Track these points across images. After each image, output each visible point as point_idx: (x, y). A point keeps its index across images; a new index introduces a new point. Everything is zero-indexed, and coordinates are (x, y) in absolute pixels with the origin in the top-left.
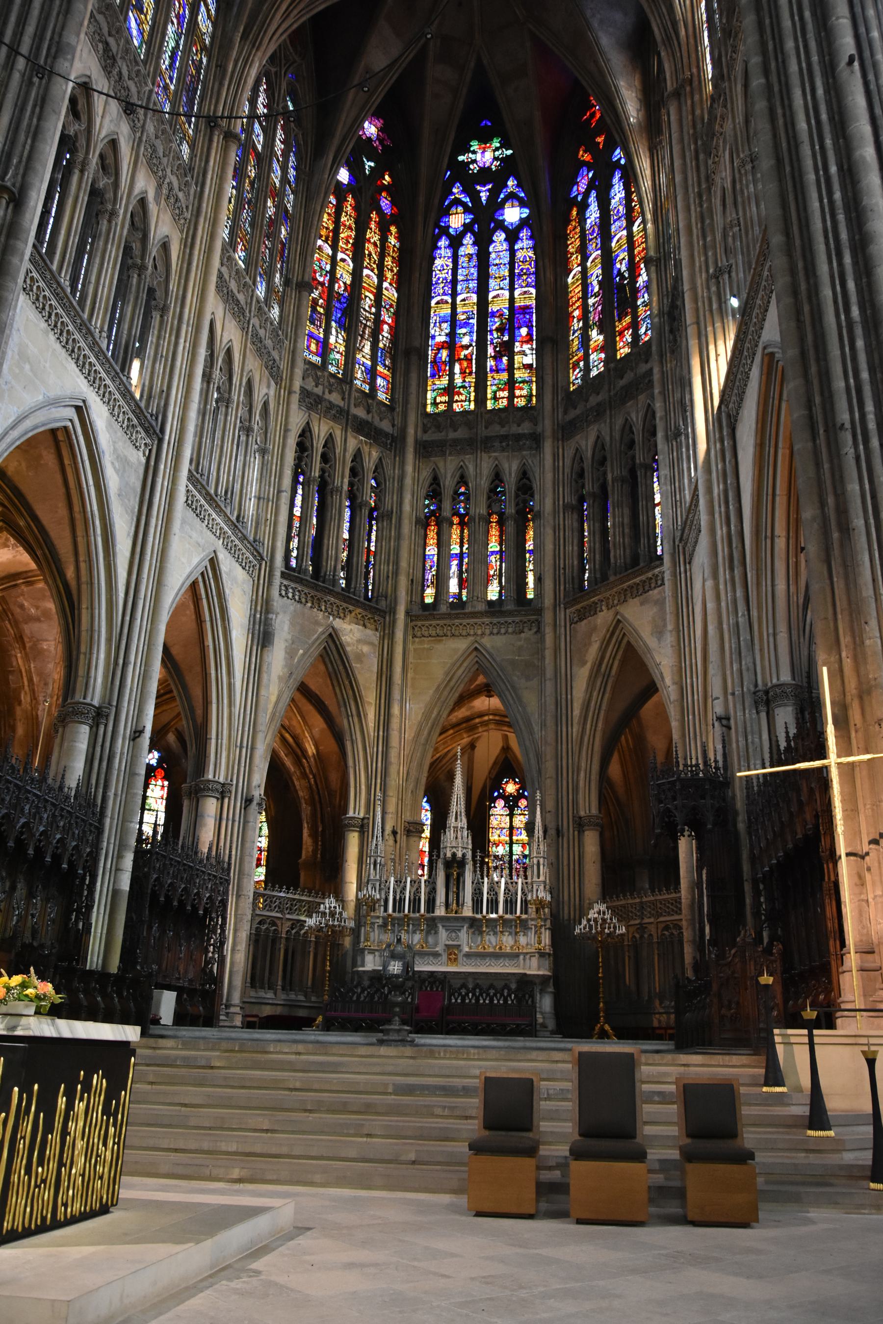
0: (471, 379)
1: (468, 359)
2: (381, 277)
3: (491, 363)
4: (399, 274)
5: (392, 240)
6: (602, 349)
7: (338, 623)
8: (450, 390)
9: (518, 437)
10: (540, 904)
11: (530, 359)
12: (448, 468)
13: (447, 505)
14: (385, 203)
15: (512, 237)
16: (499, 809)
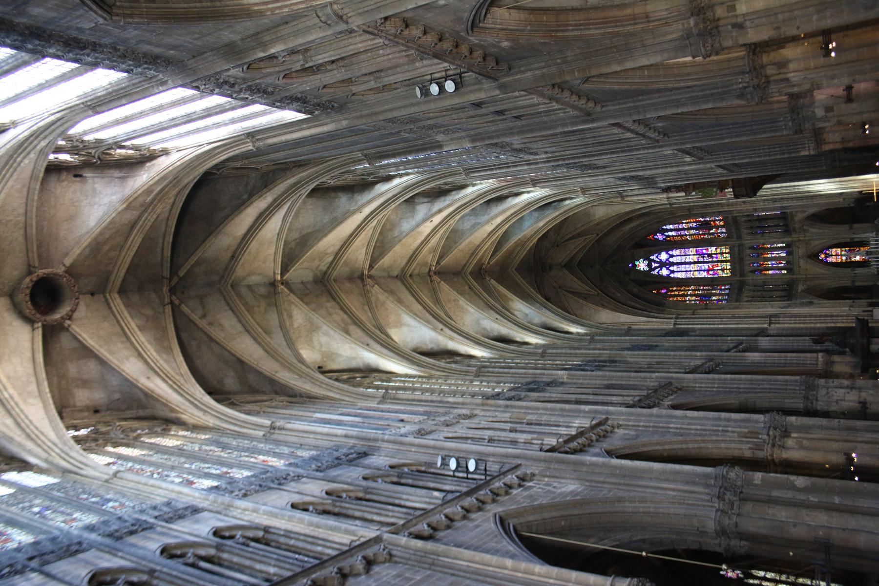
0: (719, 264)
1: (713, 266)
2: (689, 290)
3: (714, 259)
4: (685, 286)
5: (675, 289)
6: (718, 229)
7: (799, 290)
8: (723, 270)
9: (739, 250)
10: (876, 234)
11: (713, 249)
12: (747, 269)
13: (760, 268)
14: (663, 291)
15: (672, 256)
16: (830, 260)
